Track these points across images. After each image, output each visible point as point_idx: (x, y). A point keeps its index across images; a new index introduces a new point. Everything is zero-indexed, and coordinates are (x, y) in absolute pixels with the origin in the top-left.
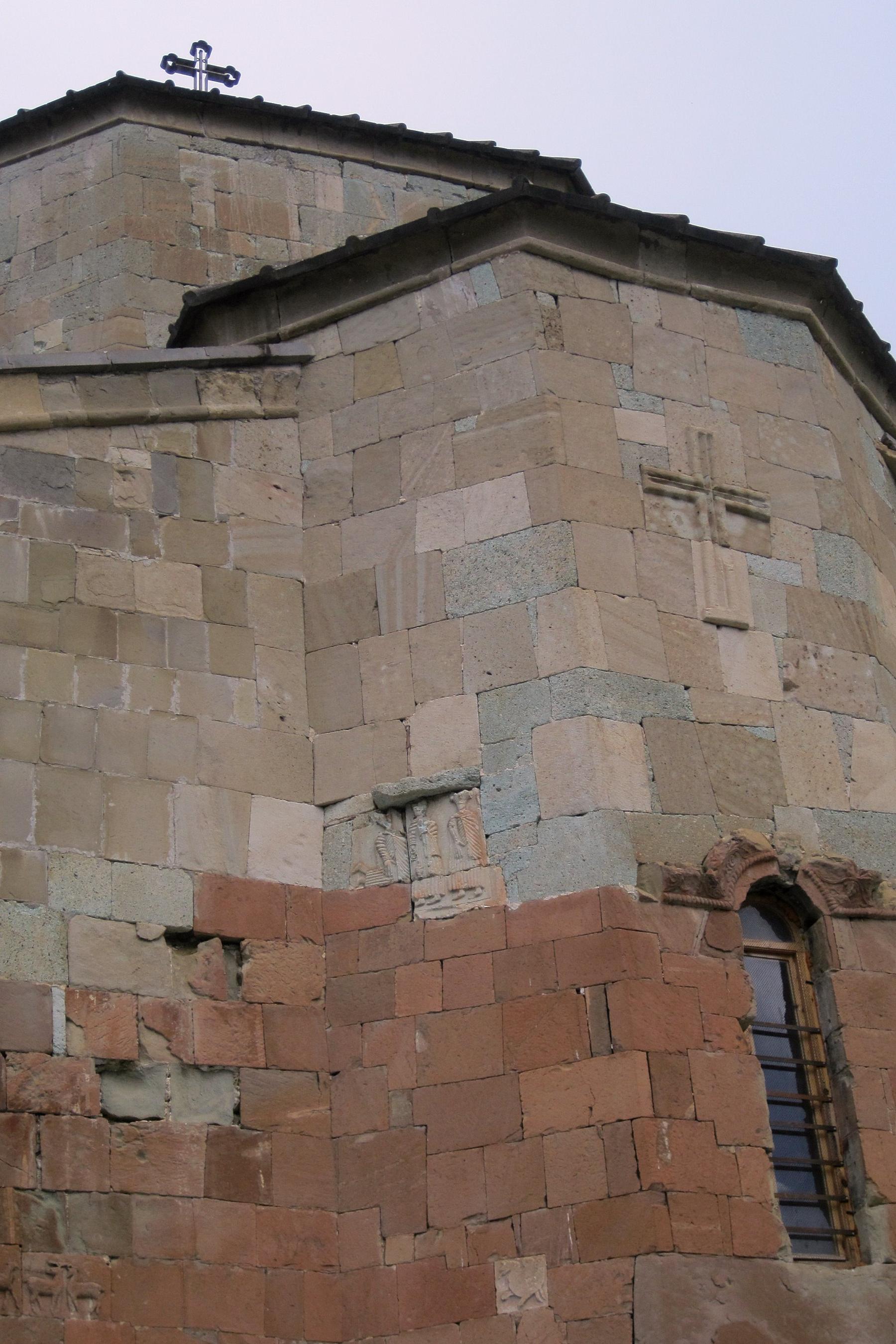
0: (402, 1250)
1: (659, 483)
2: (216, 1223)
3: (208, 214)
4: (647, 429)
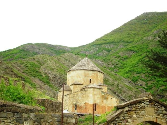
1: (95, 94)
2: (84, 109)
3: (86, 74)
4: (95, 93)
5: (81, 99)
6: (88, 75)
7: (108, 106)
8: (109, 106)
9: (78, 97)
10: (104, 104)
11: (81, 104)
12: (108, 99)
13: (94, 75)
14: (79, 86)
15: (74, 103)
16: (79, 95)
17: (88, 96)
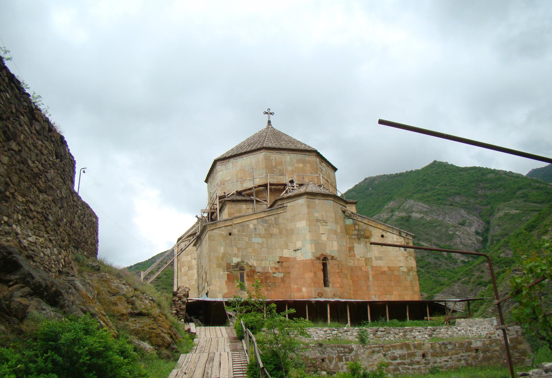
0: (296, 286)
1: (318, 220)
3: (274, 164)
4: (316, 215)
5: (261, 244)
8: (381, 267)
9: (250, 237)
10: (358, 260)
11: (264, 264)
15: (235, 260)
16: (251, 226)
17: (291, 232)
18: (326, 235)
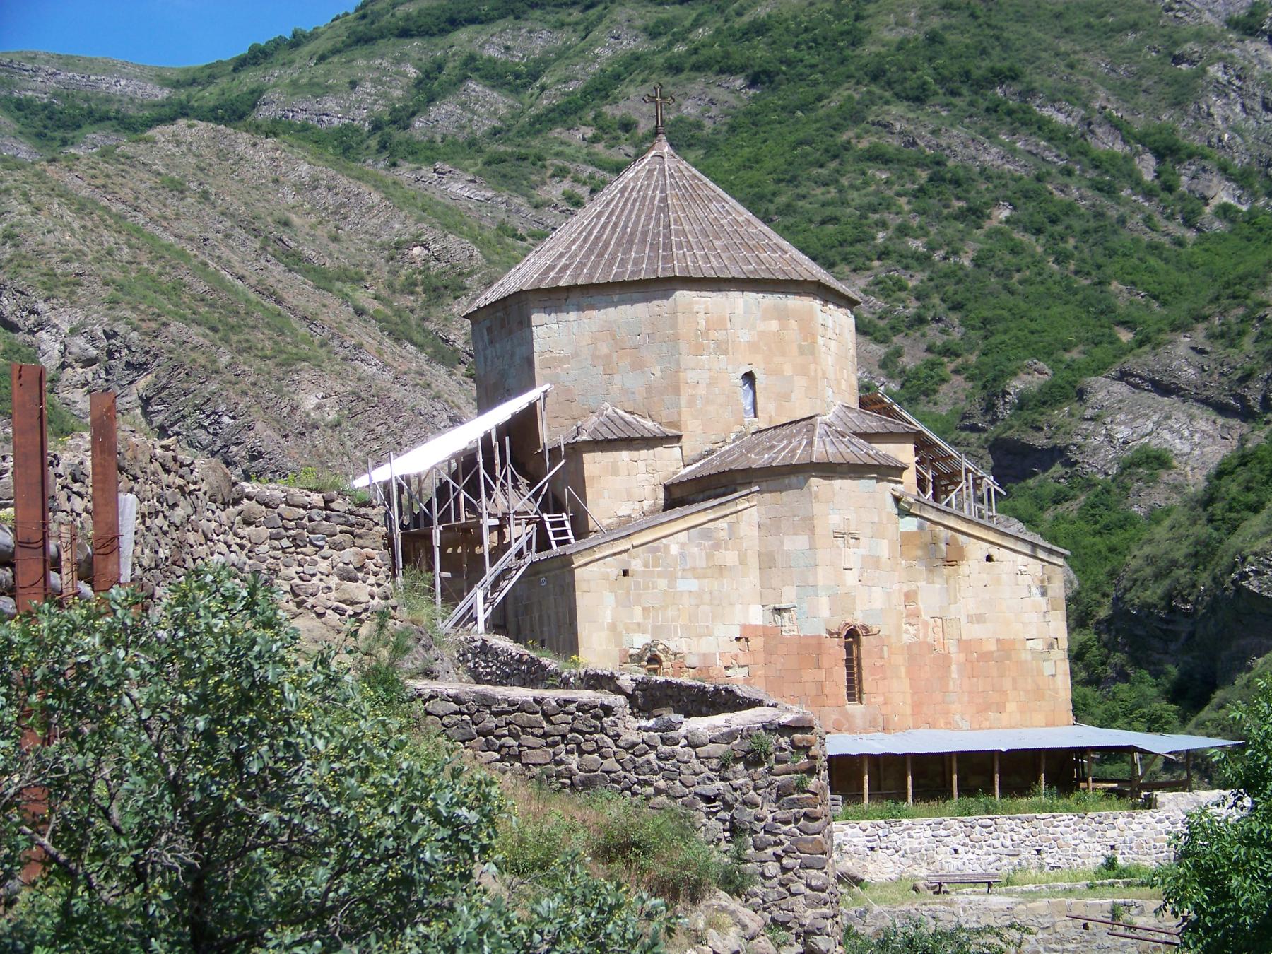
6: (714, 334)
7: (964, 645)
8: (980, 641)
9: (672, 578)
10: (926, 624)
11: (706, 645)
12: (964, 568)
13: (784, 327)
14: (643, 454)
15: (639, 641)
16: (674, 550)
18: (855, 572)
